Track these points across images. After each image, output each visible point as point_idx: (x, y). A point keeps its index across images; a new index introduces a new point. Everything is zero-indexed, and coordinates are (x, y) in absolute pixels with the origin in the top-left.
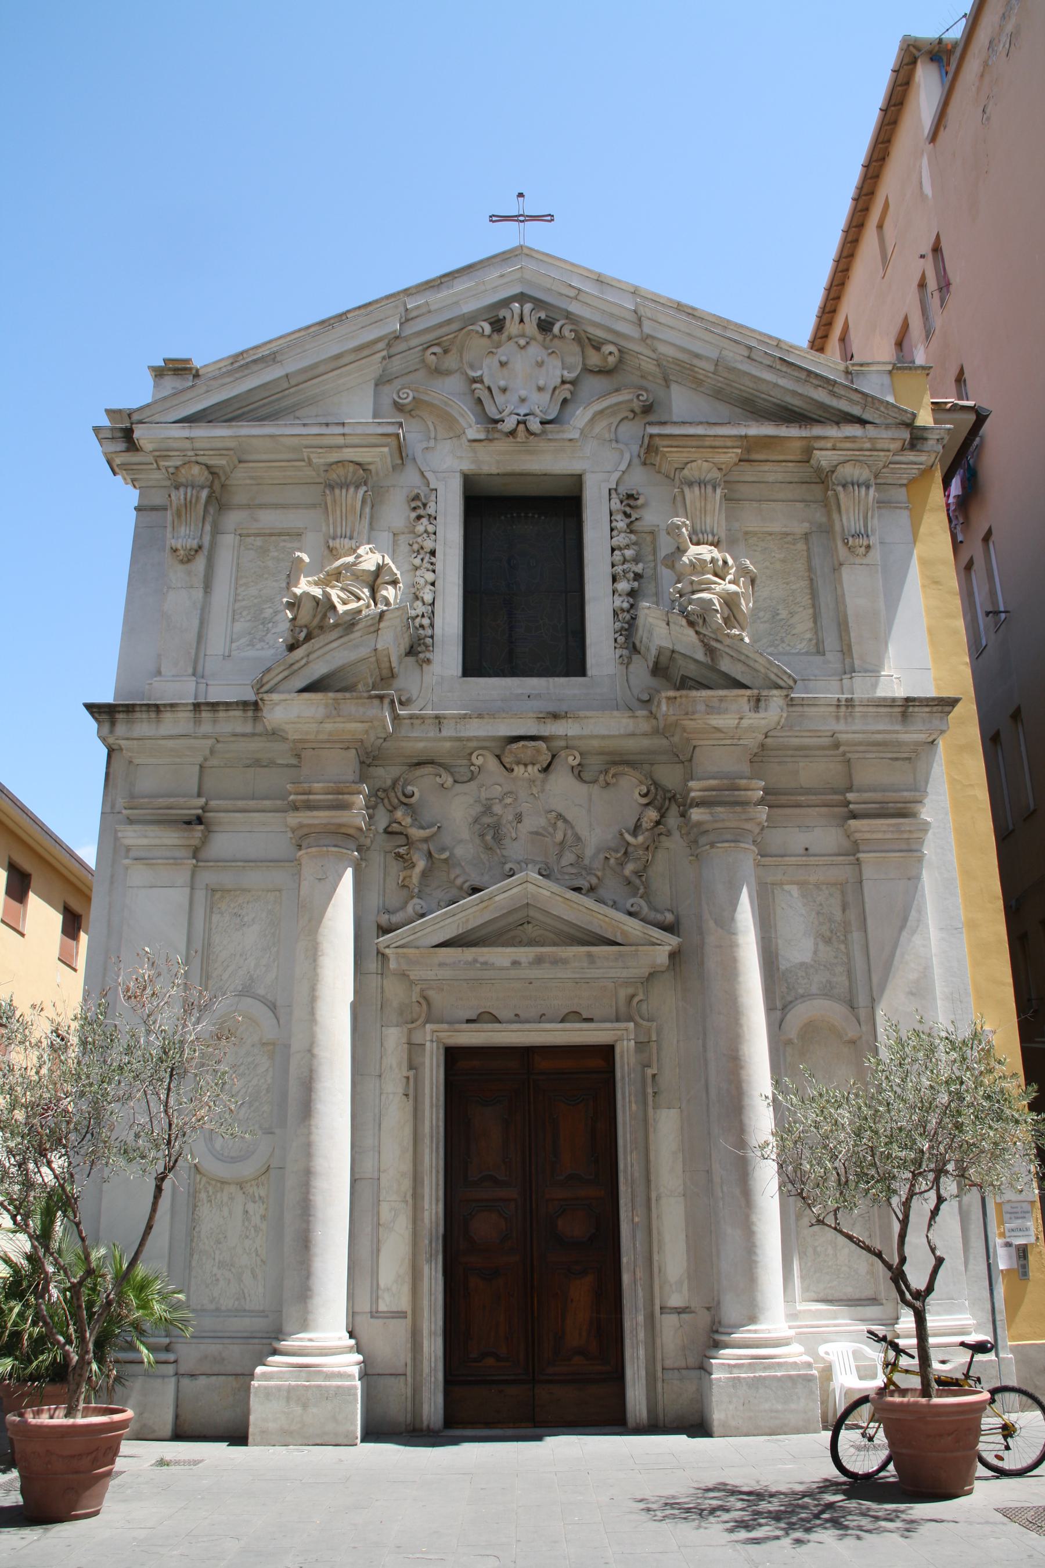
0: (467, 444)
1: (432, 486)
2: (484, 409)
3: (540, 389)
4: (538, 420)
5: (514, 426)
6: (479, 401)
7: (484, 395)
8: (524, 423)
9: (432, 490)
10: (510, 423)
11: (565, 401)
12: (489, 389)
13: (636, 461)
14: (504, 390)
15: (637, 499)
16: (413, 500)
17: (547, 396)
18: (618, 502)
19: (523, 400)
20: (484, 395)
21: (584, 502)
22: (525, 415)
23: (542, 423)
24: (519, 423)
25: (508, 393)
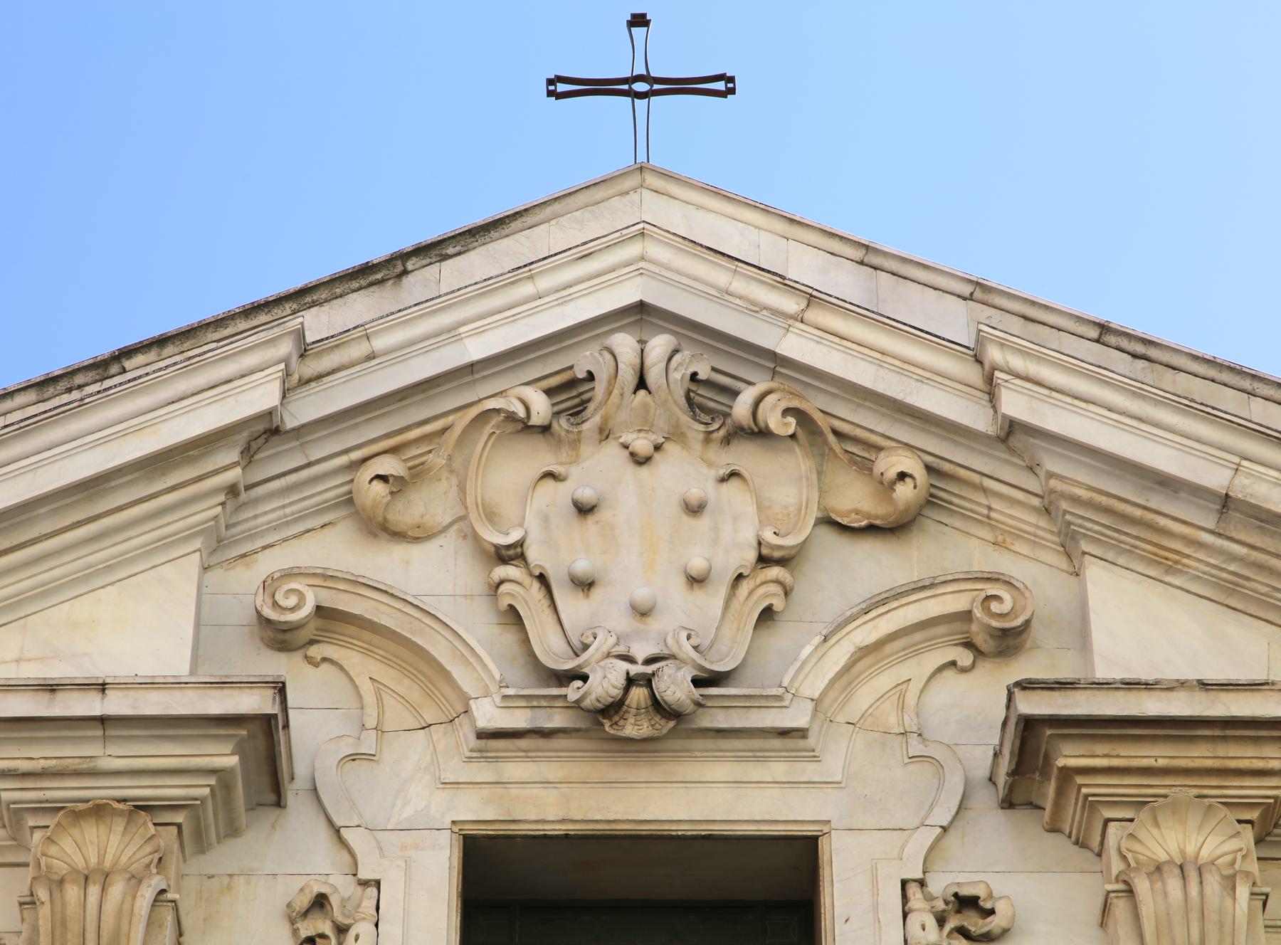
0: (473, 742)
1: (364, 874)
2: (526, 641)
3: (696, 581)
4: (687, 674)
5: (617, 693)
6: (513, 617)
7: (529, 599)
8: (648, 680)
9: (365, 884)
10: (605, 681)
11: (767, 615)
12: (542, 579)
13: (986, 800)
14: (585, 585)
15: (992, 912)
16: (305, 914)
17: (713, 600)
18: (931, 922)
19: (642, 612)
20: (529, 599)
21: (826, 923)
22: (650, 661)
23: (697, 682)
24: (631, 681)
25: (597, 593)
